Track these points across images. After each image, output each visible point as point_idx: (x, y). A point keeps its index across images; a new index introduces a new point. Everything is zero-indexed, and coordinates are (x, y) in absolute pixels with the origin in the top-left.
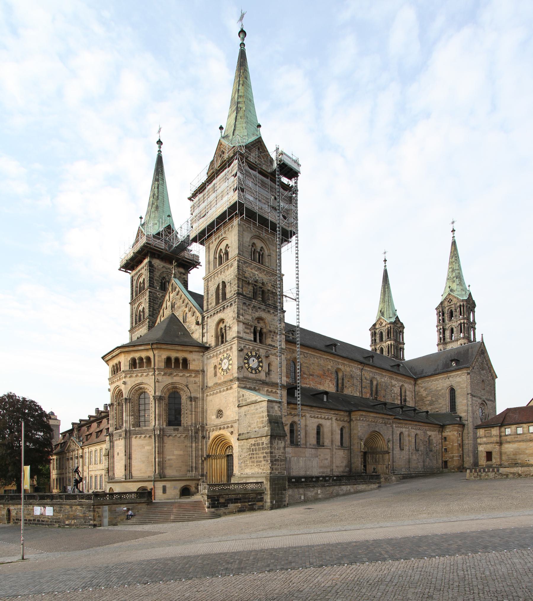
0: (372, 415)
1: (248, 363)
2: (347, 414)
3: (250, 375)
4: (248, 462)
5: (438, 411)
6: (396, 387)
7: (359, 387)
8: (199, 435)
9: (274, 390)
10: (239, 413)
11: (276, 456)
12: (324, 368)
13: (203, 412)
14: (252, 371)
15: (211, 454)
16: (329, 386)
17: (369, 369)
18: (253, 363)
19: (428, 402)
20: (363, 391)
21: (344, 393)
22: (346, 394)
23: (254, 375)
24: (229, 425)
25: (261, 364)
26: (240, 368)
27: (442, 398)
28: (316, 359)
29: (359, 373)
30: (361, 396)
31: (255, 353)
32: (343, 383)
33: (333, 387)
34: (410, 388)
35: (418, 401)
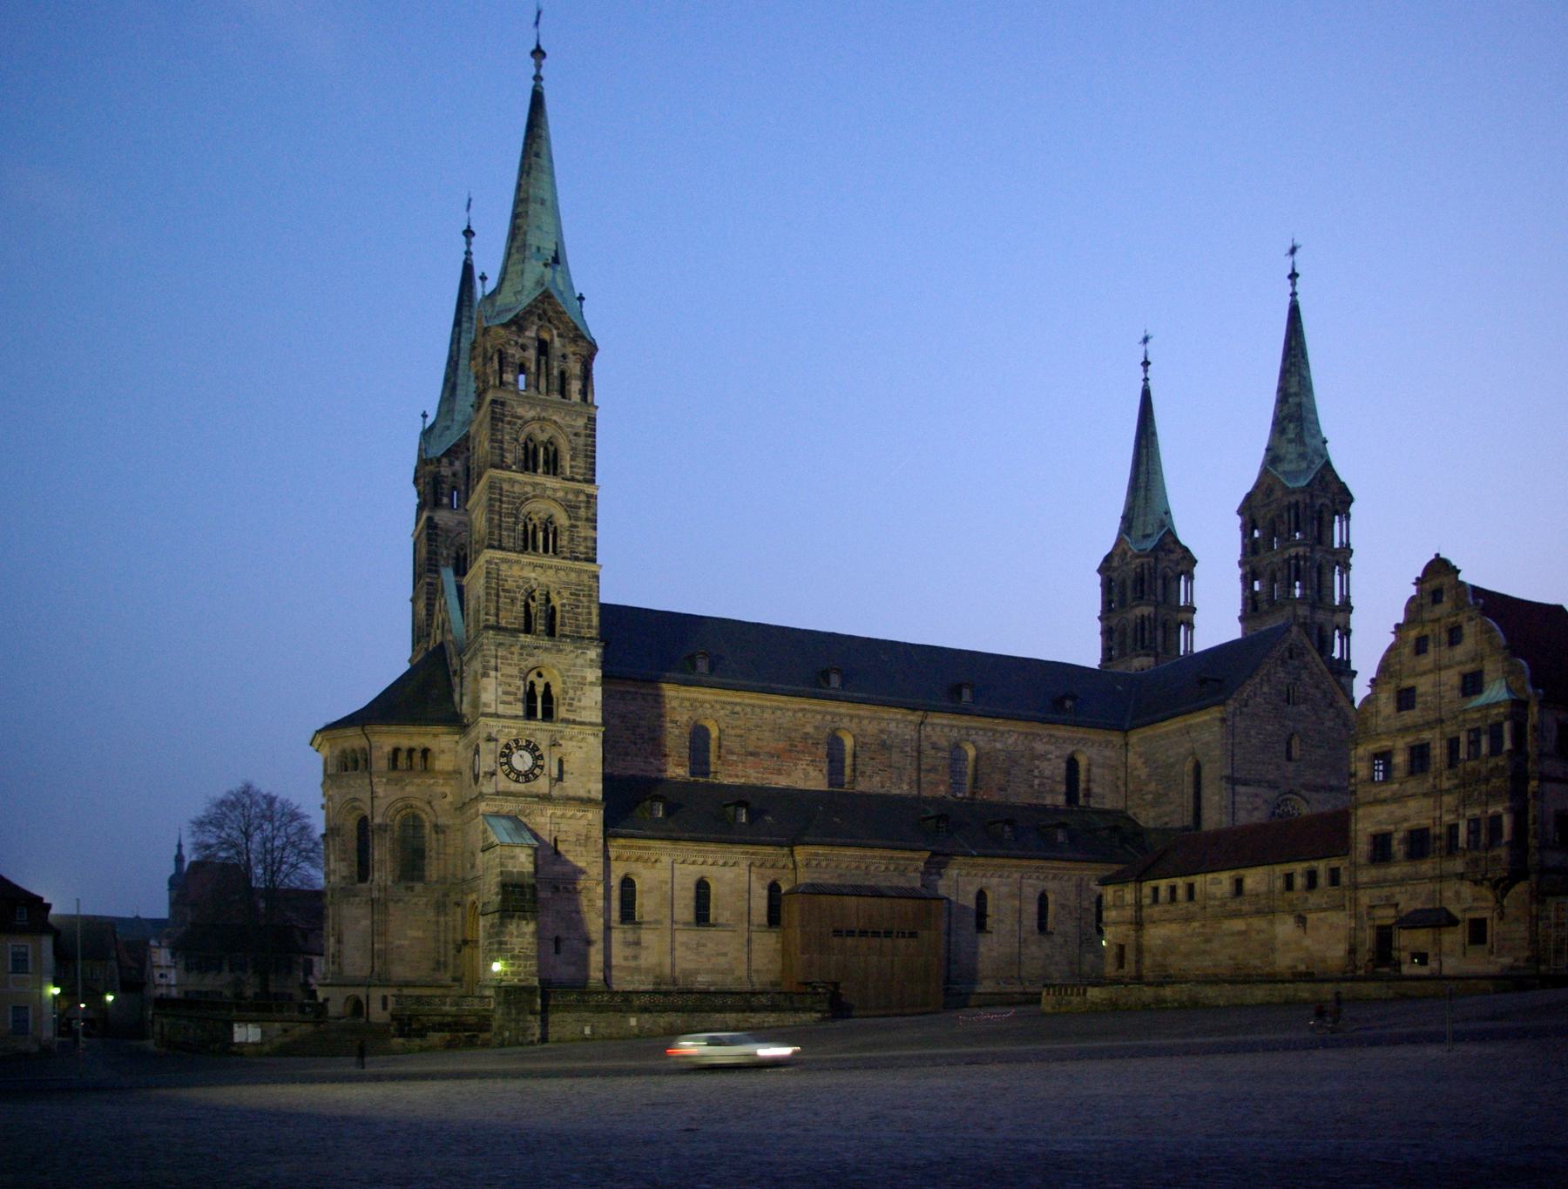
3: (515, 787)
5: (1166, 823)
6: (1049, 760)
9: (570, 813)
12: (793, 734)
16: (806, 774)
19: (1149, 797)
20: (923, 780)
33: (821, 777)
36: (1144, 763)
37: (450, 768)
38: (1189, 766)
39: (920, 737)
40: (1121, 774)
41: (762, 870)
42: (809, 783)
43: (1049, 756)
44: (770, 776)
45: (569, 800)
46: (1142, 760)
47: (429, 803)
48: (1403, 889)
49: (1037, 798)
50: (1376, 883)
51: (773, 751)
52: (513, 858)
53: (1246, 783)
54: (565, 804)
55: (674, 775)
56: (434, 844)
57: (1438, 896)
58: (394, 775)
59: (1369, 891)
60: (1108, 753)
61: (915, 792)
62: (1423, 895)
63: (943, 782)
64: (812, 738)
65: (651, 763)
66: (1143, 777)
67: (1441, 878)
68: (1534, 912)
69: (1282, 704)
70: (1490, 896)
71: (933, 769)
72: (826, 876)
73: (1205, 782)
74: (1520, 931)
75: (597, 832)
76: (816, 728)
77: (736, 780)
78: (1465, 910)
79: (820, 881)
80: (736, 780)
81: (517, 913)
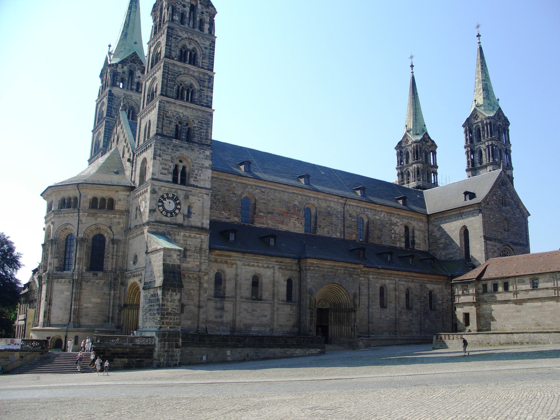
1: (163, 206)
2: (296, 261)
4: (148, 315)
6: (398, 226)
7: (340, 226)
8: (118, 282)
10: (146, 260)
11: (168, 309)
12: (289, 205)
13: (125, 256)
14: (167, 214)
15: (128, 304)
16: (295, 225)
17: (355, 204)
18: (170, 205)
19: (441, 246)
20: (346, 231)
23: (170, 218)
24: (140, 273)
25: (179, 207)
26: (152, 211)
28: (277, 194)
30: (342, 237)
31: (173, 195)
32: (316, 222)
33: (301, 226)
34: (420, 227)
36: (437, 230)
37: (123, 209)
39: (344, 211)
40: (427, 235)
41: (285, 271)
42: (296, 229)
43: (398, 224)
44: (279, 225)
45: (192, 228)
46: (437, 228)
47: (110, 227)
49: (394, 244)
51: (280, 213)
52: (170, 256)
54: (190, 230)
55: (233, 221)
56: (111, 250)
58: (93, 211)
60: (421, 224)
61: (342, 237)
63: (355, 233)
65: (223, 214)
69: (501, 205)
71: (350, 227)
73: (471, 238)
75: (206, 246)
77: (263, 226)
80: (263, 226)
81: (171, 288)
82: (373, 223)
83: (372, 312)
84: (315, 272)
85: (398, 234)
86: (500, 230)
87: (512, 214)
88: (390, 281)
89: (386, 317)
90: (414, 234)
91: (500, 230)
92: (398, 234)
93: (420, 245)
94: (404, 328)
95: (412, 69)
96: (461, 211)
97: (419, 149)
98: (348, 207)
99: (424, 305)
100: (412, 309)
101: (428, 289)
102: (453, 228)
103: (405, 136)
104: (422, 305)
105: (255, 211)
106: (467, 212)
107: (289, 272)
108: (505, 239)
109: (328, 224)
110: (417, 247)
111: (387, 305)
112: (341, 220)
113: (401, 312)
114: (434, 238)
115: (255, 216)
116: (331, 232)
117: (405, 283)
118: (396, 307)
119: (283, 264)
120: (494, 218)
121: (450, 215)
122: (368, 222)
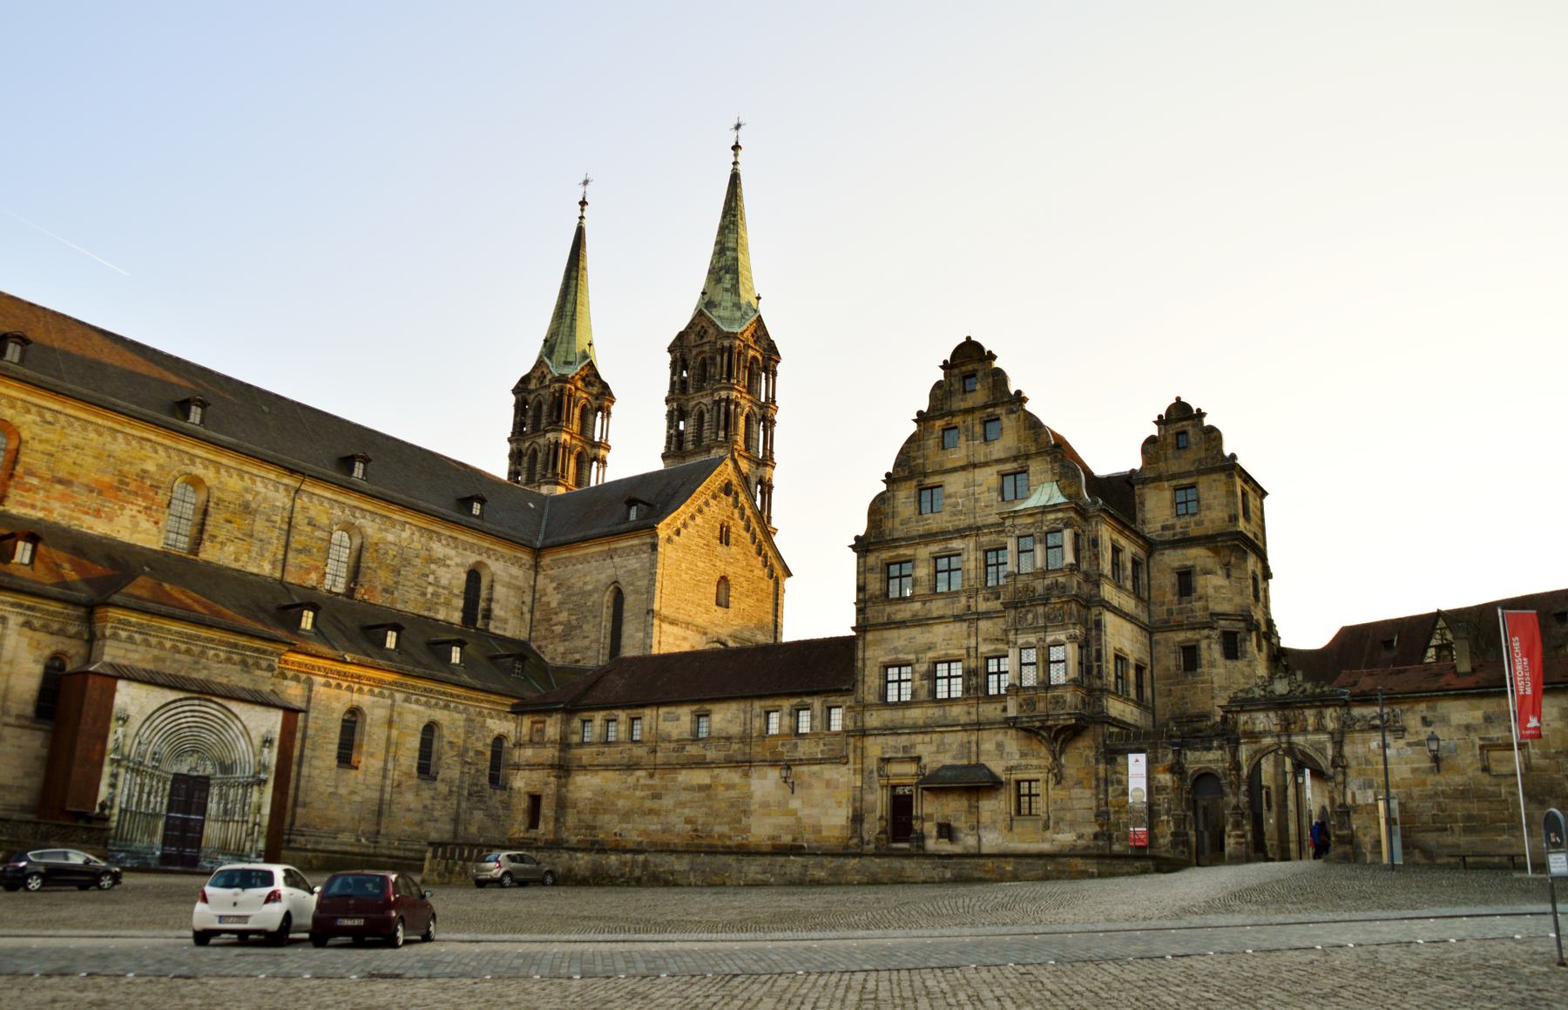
0: (175, 627)
2: (81, 612)
6: (448, 566)
7: (276, 545)
12: (126, 468)
16: (136, 525)
17: (328, 495)
19: (558, 629)
21: (203, 556)
22: (208, 563)
27: (590, 618)
28: (93, 435)
29: (281, 499)
32: (203, 524)
33: (154, 530)
34: (512, 576)
35: (538, 621)
36: (555, 589)
38: (608, 598)
39: (293, 506)
40: (528, 599)
41: (40, 636)
43: (448, 562)
46: (554, 585)
48: (927, 738)
49: (429, 610)
50: (892, 730)
51: (94, 485)
53: (673, 623)
57: (974, 748)
59: (881, 739)
60: (515, 571)
61: (278, 575)
62: (955, 746)
64: (151, 478)
66: (554, 604)
67: (979, 726)
68: (1102, 774)
70: (1044, 751)
72: (136, 656)
73: (627, 615)
74: (1083, 800)
76: (161, 467)
78: (1010, 769)
79: (126, 663)
82: (377, 551)
83: (309, 776)
84: (133, 647)
85: (444, 588)
86: (704, 602)
87: (742, 568)
88: (376, 699)
89: (353, 793)
90: (491, 594)
91: (704, 602)
92: (444, 588)
93: (505, 621)
94: (406, 827)
95: (582, 210)
96: (613, 546)
97: (566, 398)
98: (305, 499)
99: (473, 771)
100: (435, 779)
101: (492, 731)
102: (589, 587)
103: (540, 363)
104: (466, 770)
105: (14, 469)
106: (624, 548)
107: (54, 638)
108: (716, 625)
109: (240, 536)
110: (496, 627)
111: (359, 762)
112: (280, 529)
113: (399, 786)
114: (544, 608)
115: (12, 483)
116: (244, 557)
117: (422, 708)
118: (385, 769)
119: (39, 615)
120: (692, 570)
121: (588, 554)
122: (362, 546)
